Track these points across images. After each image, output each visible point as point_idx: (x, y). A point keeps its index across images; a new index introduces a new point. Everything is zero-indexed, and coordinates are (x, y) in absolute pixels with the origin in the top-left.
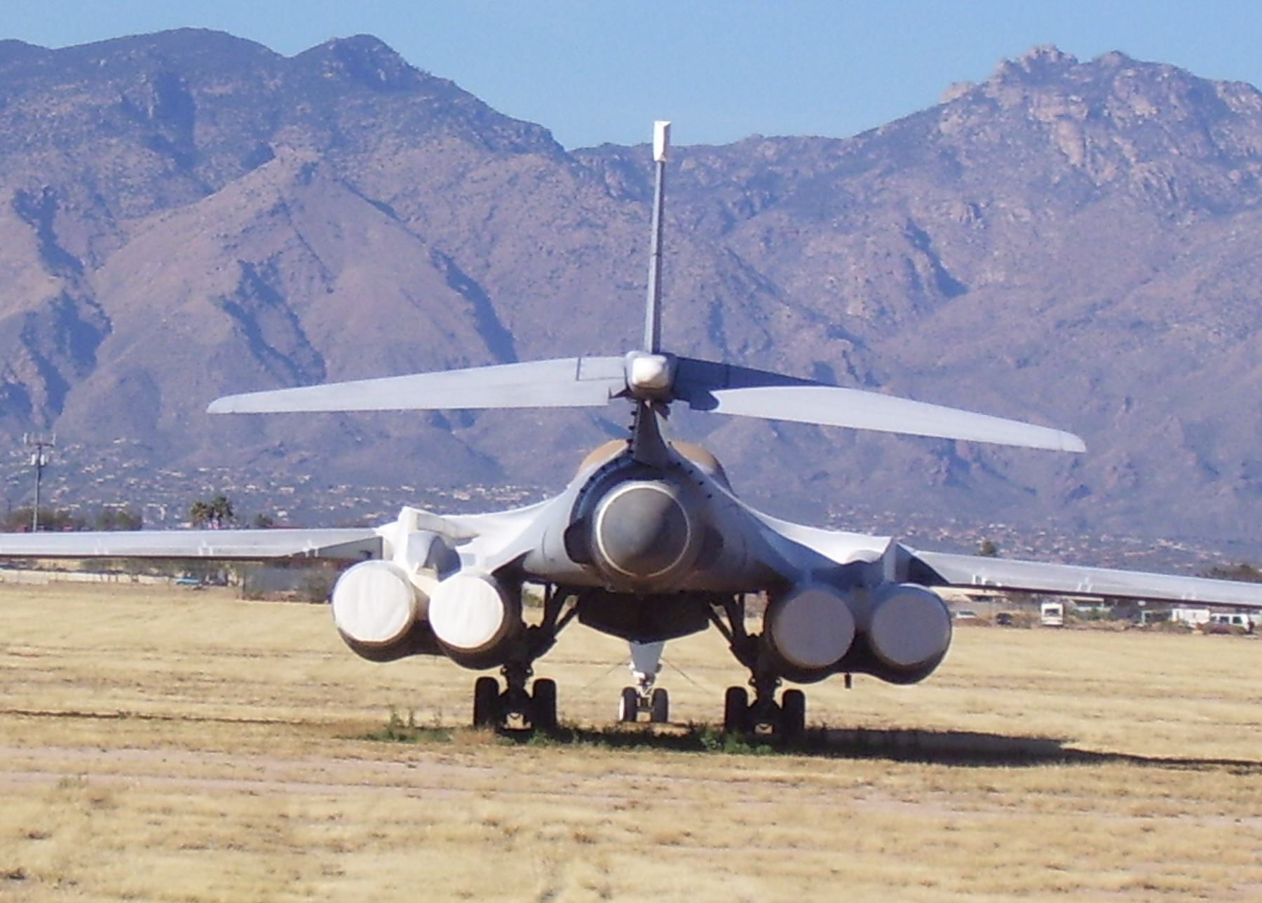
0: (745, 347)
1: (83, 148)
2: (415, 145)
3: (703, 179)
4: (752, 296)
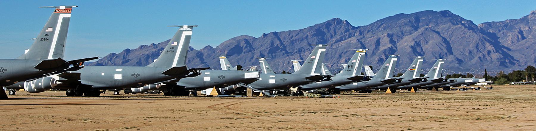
0: (481, 49)
1: (402, 27)
2: (445, 24)
3: (499, 26)
4: (484, 42)
